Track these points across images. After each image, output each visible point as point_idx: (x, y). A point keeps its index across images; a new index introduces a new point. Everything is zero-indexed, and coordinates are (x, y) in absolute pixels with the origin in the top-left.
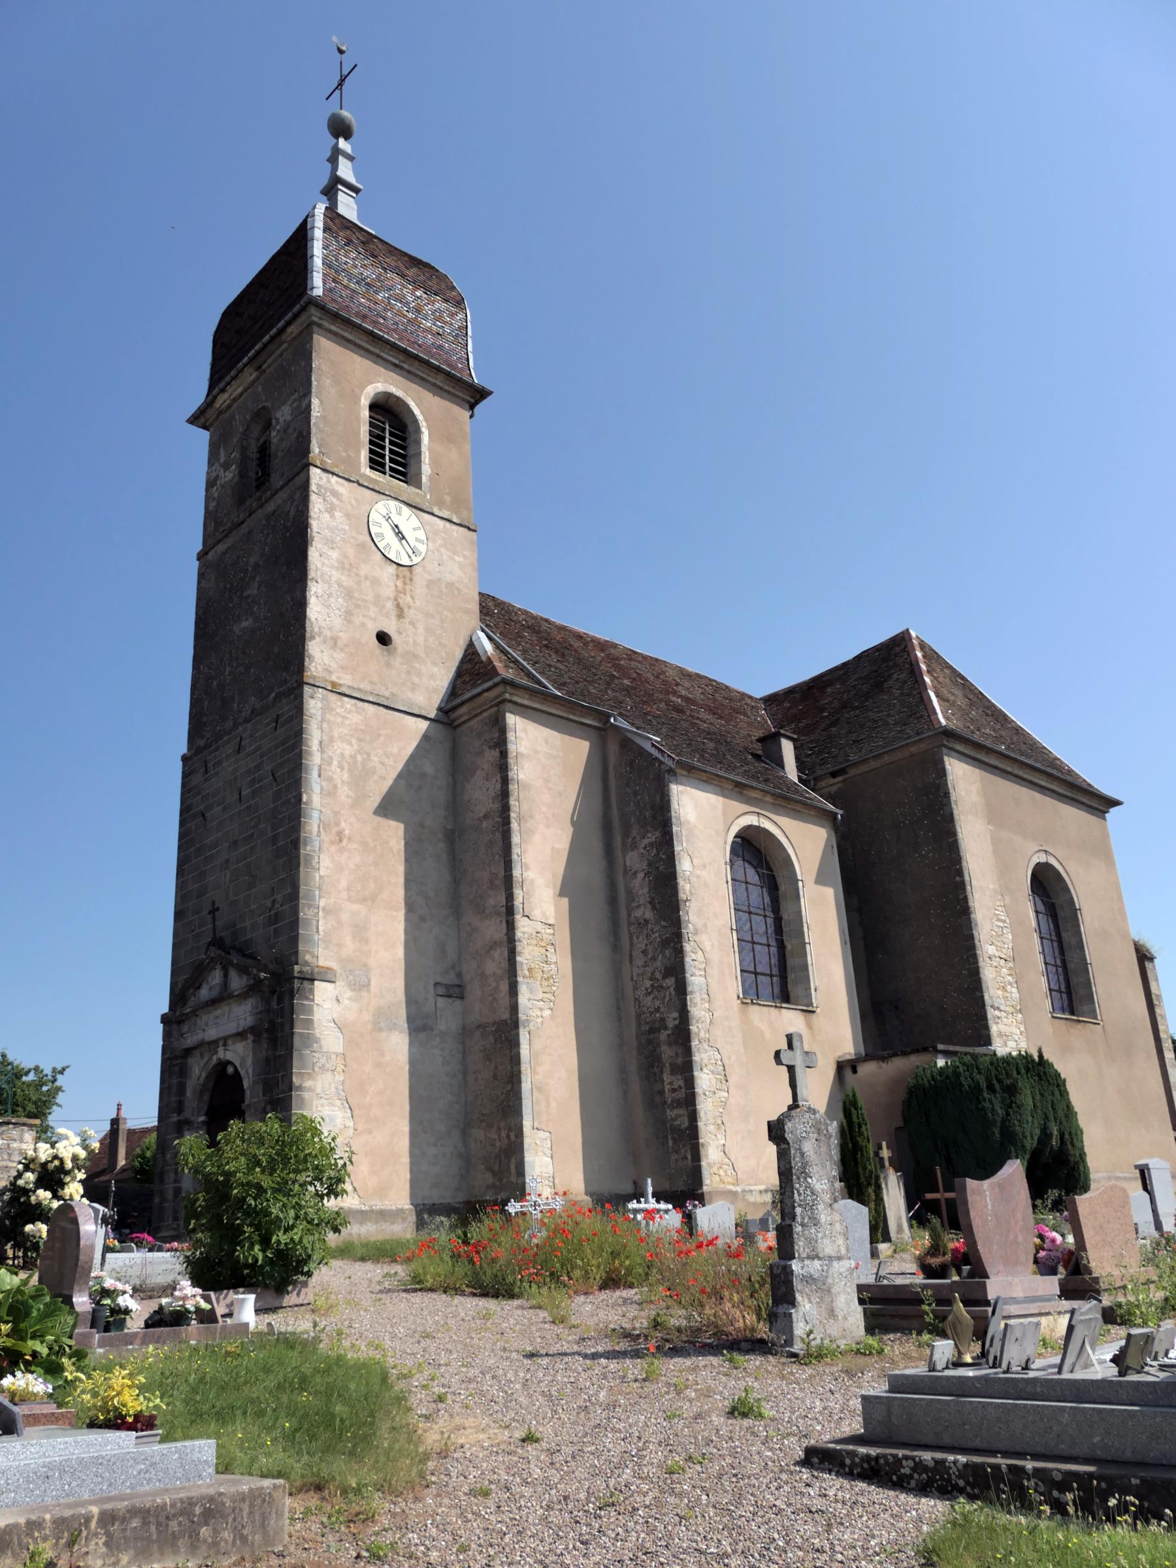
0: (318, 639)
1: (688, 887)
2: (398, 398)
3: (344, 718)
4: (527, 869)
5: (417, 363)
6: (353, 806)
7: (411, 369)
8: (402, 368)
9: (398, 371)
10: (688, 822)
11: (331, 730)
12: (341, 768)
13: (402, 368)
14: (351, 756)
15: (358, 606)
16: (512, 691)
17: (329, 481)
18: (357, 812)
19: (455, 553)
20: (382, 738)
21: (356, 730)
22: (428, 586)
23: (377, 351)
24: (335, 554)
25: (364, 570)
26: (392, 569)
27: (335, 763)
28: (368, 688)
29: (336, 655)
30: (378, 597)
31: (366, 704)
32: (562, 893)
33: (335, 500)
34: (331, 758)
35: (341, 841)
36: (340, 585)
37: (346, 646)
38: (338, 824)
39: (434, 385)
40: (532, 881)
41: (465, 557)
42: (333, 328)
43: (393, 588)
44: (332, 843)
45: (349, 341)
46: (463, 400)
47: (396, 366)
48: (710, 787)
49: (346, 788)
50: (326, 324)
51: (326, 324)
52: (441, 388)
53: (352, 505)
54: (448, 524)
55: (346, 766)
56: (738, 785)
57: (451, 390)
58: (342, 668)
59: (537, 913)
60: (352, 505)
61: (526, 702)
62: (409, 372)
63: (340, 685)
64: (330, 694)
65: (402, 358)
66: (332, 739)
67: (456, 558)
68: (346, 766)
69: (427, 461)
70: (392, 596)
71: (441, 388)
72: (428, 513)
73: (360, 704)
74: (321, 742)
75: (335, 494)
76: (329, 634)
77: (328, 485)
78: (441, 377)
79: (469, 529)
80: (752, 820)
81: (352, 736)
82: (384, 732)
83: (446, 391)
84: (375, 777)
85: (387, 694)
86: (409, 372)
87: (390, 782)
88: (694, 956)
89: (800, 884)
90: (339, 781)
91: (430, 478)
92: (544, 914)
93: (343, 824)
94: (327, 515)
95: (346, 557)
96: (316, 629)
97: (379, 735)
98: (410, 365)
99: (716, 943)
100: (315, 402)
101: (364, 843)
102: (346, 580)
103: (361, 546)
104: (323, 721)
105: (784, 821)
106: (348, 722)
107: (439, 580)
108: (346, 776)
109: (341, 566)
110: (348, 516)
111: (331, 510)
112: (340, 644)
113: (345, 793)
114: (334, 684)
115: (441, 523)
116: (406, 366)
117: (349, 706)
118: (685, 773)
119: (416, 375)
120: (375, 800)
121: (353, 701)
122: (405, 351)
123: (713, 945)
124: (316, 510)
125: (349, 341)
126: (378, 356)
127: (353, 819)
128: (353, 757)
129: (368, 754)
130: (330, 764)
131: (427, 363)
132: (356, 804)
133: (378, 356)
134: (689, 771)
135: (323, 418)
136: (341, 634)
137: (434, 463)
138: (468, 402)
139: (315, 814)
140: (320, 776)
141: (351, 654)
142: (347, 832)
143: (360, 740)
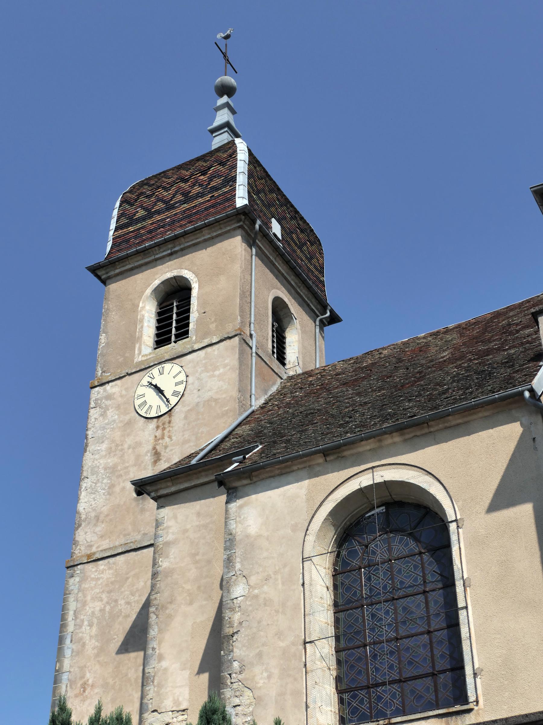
0: (83, 524)
1: (237, 617)
2: (175, 278)
3: (98, 579)
4: (161, 658)
5: (182, 239)
6: (97, 655)
7: (182, 246)
8: (176, 252)
9: (174, 256)
10: (248, 536)
11: (85, 596)
12: (91, 625)
13: (176, 252)
14: (100, 610)
15: (121, 476)
16: (154, 488)
17: (105, 390)
18: (101, 659)
19: (216, 368)
20: (130, 580)
21: (107, 585)
22: (186, 418)
23: (153, 258)
24: (104, 446)
25: (129, 441)
26: (152, 425)
27: (86, 623)
28: (123, 541)
29: (98, 529)
30: (138, 457)
31: (118, 557)
32: (201, 671)
33: (108, 403)
34: (83, 621)
35: (84, 691)
36: (105, 469)
37: (107, 515)
38: (82, 677)
39: (205, 240)
40: (166, 669)
41: (225, 366)
42: (117, 271)
43: (152, 439)
44: (76, 696)
45: (132, 269)
46: (234, 229)
47: (171, 254)
48: (290, 477)
49: (93, 641)
50: (112, 273)
51: (112, 273)
52: (212, 238)
53: (121, 396)
54: (209, 349)
55: (95, 621)
56: (325, 453)
57: (219, 232)
58: (102, 537)
59: (168, 704)
60: (121, 396)
61: (173, 489)
62: (182, 250)
63: (94, 553)
64: (86, 566)
65: (170, 246)
66: (84, 604)
67: (217, 373)
68: (95, 621)
69: (196, 308)
70: (150, 447)
71: (212, 238)
72: (190, 353)
73: (111, 560)
74: (75, 611)
75: (109, 397)
76: (93, 514)
77: (105, 394)
78: (205, 231)
79: (230, 338)
80: (365, 480)
81: (103, 592)
82: (132, 573)
83: (217, 236)
84: (121, 619)
85: (139, 537)
86: (182, 250)
87: (134, 616)
88: (237, 701)
89: (453, 527)
90: (88, 638)
91: (199, 321)
92: (177, 702)
93: (88, 675)
94: (101, 418)
95: (113, 441)
96: (83, 517)
97: (128, 578)
98: (180, 245)
99: (276, 672)
100: (103, 338)
101: (105, 685)
102: (111, 461)
103: (129, 423)
104: (79, 590)
105: (430, 455)
106: (99, 582)
107: (197, 404)
108: (94, 630)
109: (110, 451)
110: (118, 407)
111: (103, 415)
112: (102, 517)
113: (91, 645)
114: (89, 556)
115: (201, 353)
116: (177, 249)
117: (102, 567)
118: (245, 482)
119: (189, 247)
120: (119, 638)
121: (106, 561)
122: (166, 241)
123: (269, 677)
124: (93, 420)
125: (132, 269)
126: (156, 260)
127: (97, 667)
128: (102, 610)
129: (116, 601)
130: (81, 626)
131: (185, 234)
132: (101, 650)
133: (156, 260)
134: (250, 477)
135: (107, 344)
136: (102, 509)
137: (202, 303)
138: (239, 227)
139: (65, 677)
140: (71, 641)
141: (111, 520)
142: (90, 682)
143: (109, 592)
